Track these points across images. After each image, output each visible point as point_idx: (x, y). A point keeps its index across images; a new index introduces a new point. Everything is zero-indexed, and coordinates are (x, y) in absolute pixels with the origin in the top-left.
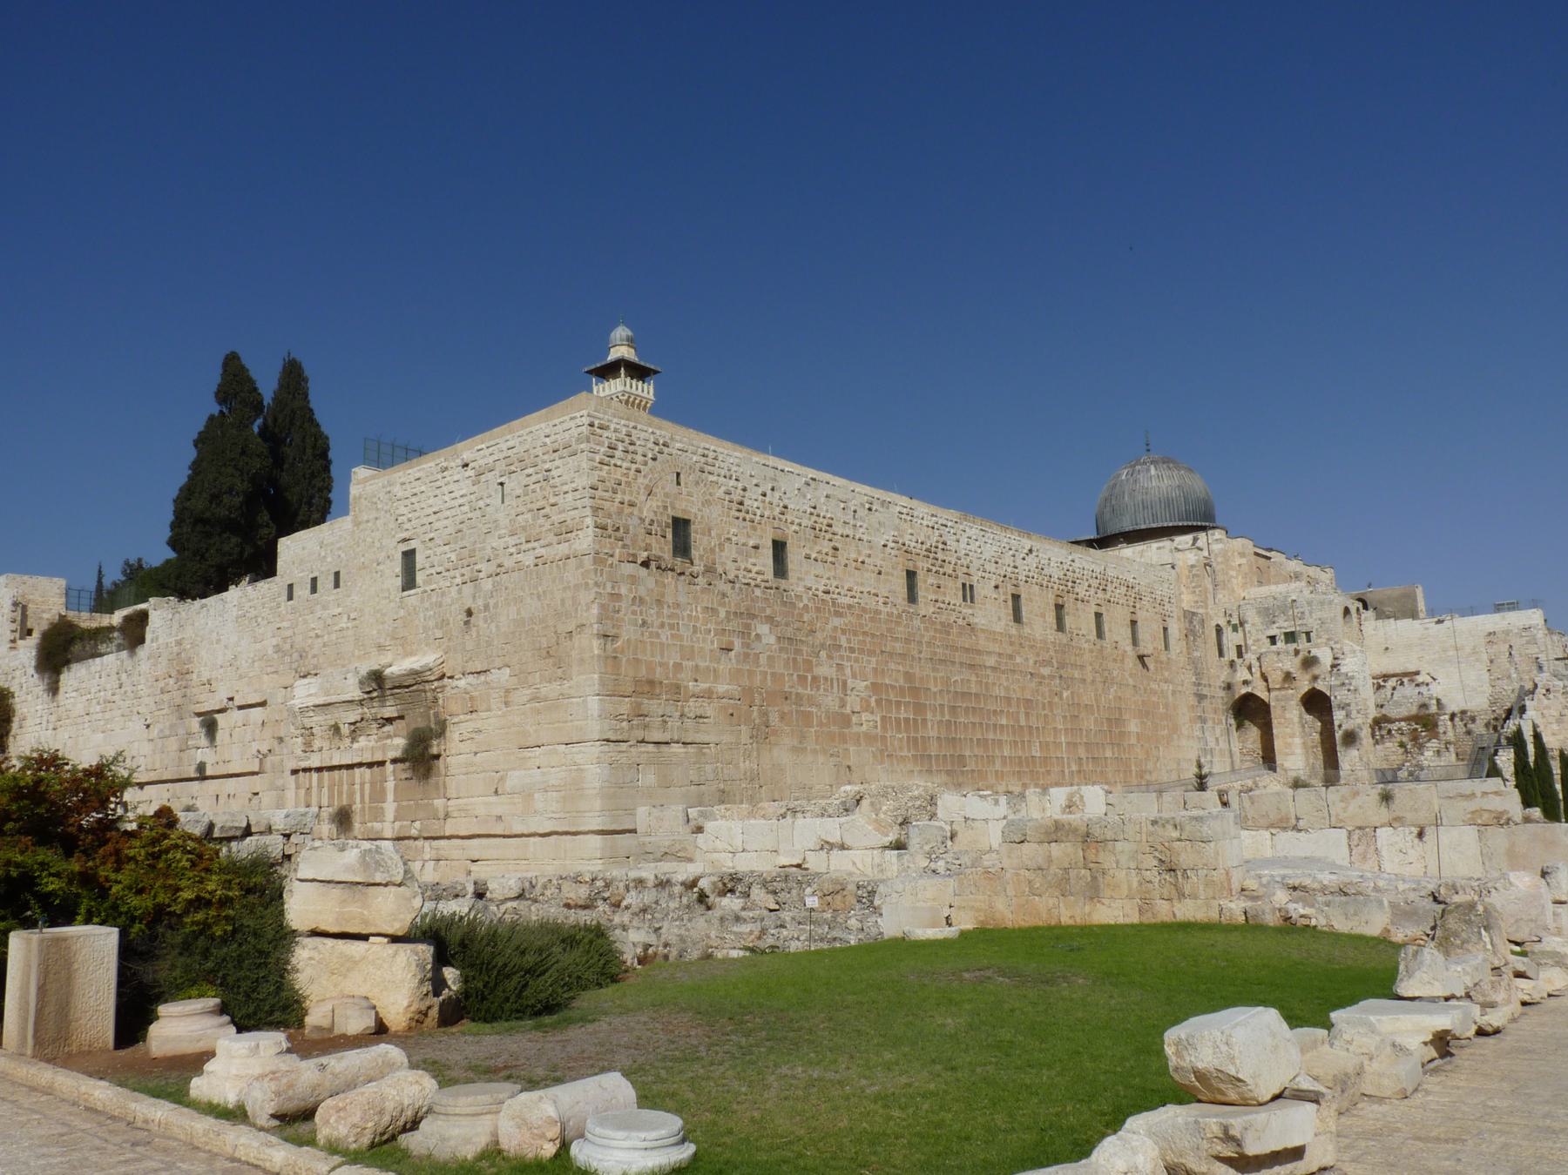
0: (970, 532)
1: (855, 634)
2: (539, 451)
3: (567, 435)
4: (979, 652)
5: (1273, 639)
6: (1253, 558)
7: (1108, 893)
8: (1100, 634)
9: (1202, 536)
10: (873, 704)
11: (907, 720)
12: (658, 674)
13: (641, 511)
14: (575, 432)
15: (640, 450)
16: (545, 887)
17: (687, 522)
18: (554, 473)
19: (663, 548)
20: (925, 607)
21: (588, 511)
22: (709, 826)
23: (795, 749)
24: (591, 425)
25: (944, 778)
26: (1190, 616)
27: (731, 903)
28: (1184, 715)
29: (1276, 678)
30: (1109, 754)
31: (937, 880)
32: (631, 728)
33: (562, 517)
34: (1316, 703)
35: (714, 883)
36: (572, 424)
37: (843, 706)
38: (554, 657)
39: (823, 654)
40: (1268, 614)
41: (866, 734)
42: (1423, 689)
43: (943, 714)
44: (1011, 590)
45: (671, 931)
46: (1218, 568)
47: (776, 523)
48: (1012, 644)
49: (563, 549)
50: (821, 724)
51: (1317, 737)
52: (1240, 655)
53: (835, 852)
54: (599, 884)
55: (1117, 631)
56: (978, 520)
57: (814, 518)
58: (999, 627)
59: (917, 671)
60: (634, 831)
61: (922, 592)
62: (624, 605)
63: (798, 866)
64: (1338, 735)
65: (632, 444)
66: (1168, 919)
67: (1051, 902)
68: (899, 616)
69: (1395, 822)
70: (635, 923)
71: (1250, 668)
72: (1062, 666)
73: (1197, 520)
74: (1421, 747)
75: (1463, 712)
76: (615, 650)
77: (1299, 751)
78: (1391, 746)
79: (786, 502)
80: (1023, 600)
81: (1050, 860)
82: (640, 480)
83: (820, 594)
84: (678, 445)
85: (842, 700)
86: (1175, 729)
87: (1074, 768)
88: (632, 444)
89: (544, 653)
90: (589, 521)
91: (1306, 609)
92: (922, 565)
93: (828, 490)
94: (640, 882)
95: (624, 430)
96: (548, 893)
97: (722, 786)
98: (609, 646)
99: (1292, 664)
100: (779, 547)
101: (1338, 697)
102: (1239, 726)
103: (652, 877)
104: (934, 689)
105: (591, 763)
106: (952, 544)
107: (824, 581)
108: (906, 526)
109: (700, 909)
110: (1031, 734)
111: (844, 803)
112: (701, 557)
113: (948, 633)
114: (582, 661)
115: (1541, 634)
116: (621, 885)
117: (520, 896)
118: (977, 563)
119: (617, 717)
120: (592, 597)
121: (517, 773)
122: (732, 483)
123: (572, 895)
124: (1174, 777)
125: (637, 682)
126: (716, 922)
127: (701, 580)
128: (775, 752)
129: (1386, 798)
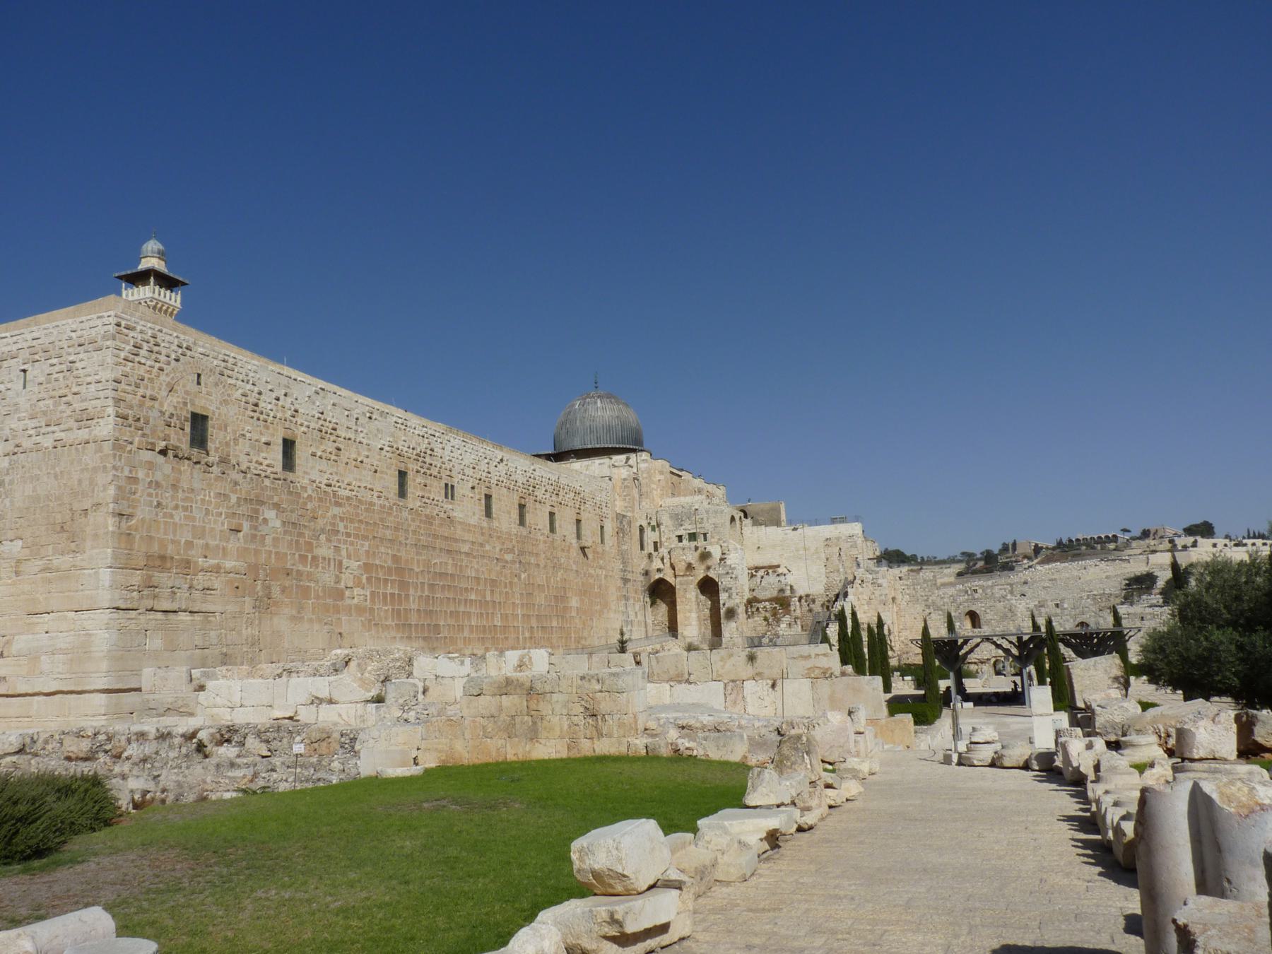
0: (454, 442)
1: (352, 521)
2: (65, 344)
3: (93, 331)
4: (456, 540)
5: (680, 538)
6: (669, 475)
7: (544, 734)
8: (552, 529)
9: (633, 456)
10: (364, 581)
11: (392, 595)
12: (170, 550)
13: (161, 404)
14: (102, 330)
15: (164, 351)
16: (46, 742)
18: (78, 365)
19: (181, 439)
20: (412, 501)
21: (110, 402)
22: (210, 685)
23: (293, 618)
24: (118, 325)
25: (421, 643)
26: (620, 517)
27: (228, 752)
28: (613, 593)
29: (681, 567)
30: (554, 624)
31: (408, 727)
32: (142, 598)
33: (84, 405)
34: (709, 587)
35: (212, 735)
36: (99, 322)
37: (338, 582)
38: (68, 532)
39: (323, 537)
40: (678, 519)
41: (357, 606)
42: (782, 578)
43: (423, 591)
44: (484, 491)
45: (169, 778)
46: (643, 482)
47: (287, 424)
48: (483, 534)
49: (83, 434)
50: (317, 597)
51: (707, 612)
52: (656, 549)
53: (324, 705)
54: (102, 737)
55: (566, 527)
56: (461, 433)
57: (321, 422)
58: (473, 521)
59: (403, 554)
60: (139, 690)
61: (410, 489)
62: (140, 487)
63: (291, 718)
64: (723, 611)
65: (157, 345)
66: (589, 754)
67: (500, 742)
68: (391, 508)
69: (757, 677)
70: (135, 772)
71: (662, 559)
72: (521, 553)
73: (629, 444)
74: (778, 621)
75: (807, 596)
76: (129, 528)
77: (694, 622)
78: (758, 619)
79: (297, 406)
80: (494, 500)
81: (500, 709)
82: (163, 377)
83: (323, 486)
84: (200, 350)
85: (337, 577)
86: (605, 605)
87: (527, 635)
88: (157, 345)
89: (59, 529)
90: (111, 410)
91: (705, 516)
92: (412, 467)
93: (334, 399)
94: (142, 736)
95: (150, 332)
96: (49, 747)
97: (224, 650)
98: (123, 524)
99: (692, 557)
100: (288, 445)
101: (724, 582)
102: (653, 604)
103: (154, 731)
104: (417, 570)
105: (101, 631)
106: (438, 451)
107: (326, 476)
108: (401, 434)
109: (199, 757)
110: (494, 607)
111: (334, 664)
112: (217, 449)
113: (431, 524)
114: (96, 536)
115: (860, 541)
116: (123, 738)
117: (21, 751)
118: (457, 468)
119: (128, 588)
120: (110, 478)
121: (24, 637)
122: (249, 387)
123: (74, 748)
124: (603, 642)
125: (149, 557)
126: (212, 769)
127: (215, 467)
128: (276, 620)
129: (752, 658)
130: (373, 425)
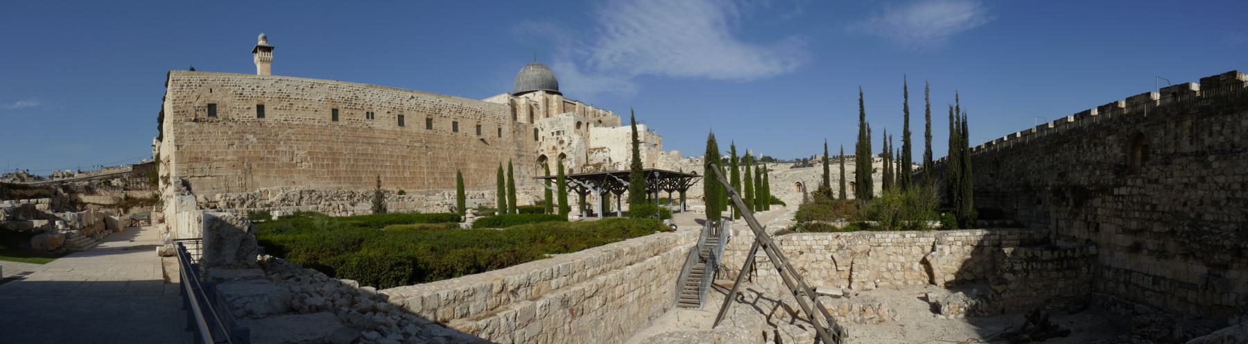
17: (215, 105)
19: (203, 115)
44: (397, 113)
59: (335, 147)
92: (341, 107)
106: (361, 96)
130: (314, 91)
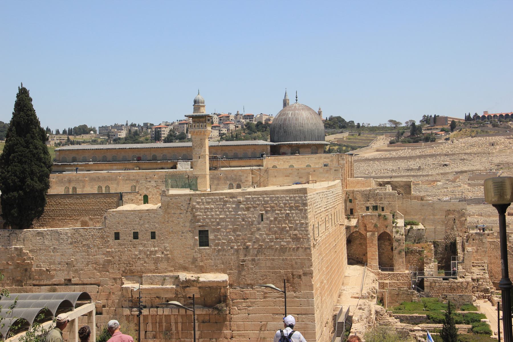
64: (395, 252)
